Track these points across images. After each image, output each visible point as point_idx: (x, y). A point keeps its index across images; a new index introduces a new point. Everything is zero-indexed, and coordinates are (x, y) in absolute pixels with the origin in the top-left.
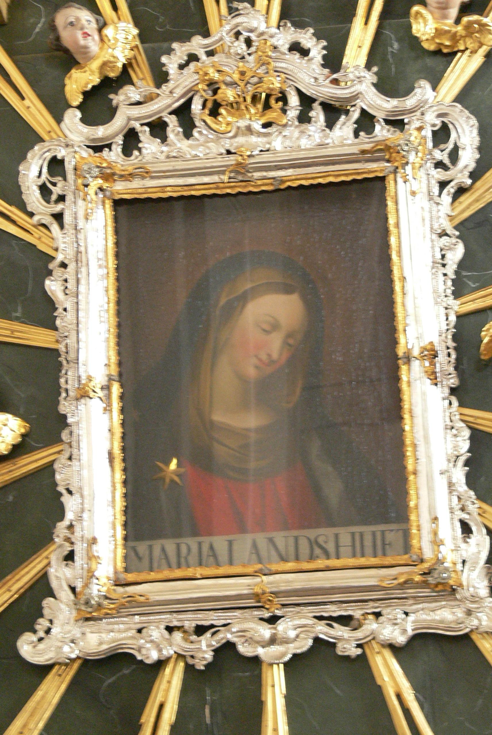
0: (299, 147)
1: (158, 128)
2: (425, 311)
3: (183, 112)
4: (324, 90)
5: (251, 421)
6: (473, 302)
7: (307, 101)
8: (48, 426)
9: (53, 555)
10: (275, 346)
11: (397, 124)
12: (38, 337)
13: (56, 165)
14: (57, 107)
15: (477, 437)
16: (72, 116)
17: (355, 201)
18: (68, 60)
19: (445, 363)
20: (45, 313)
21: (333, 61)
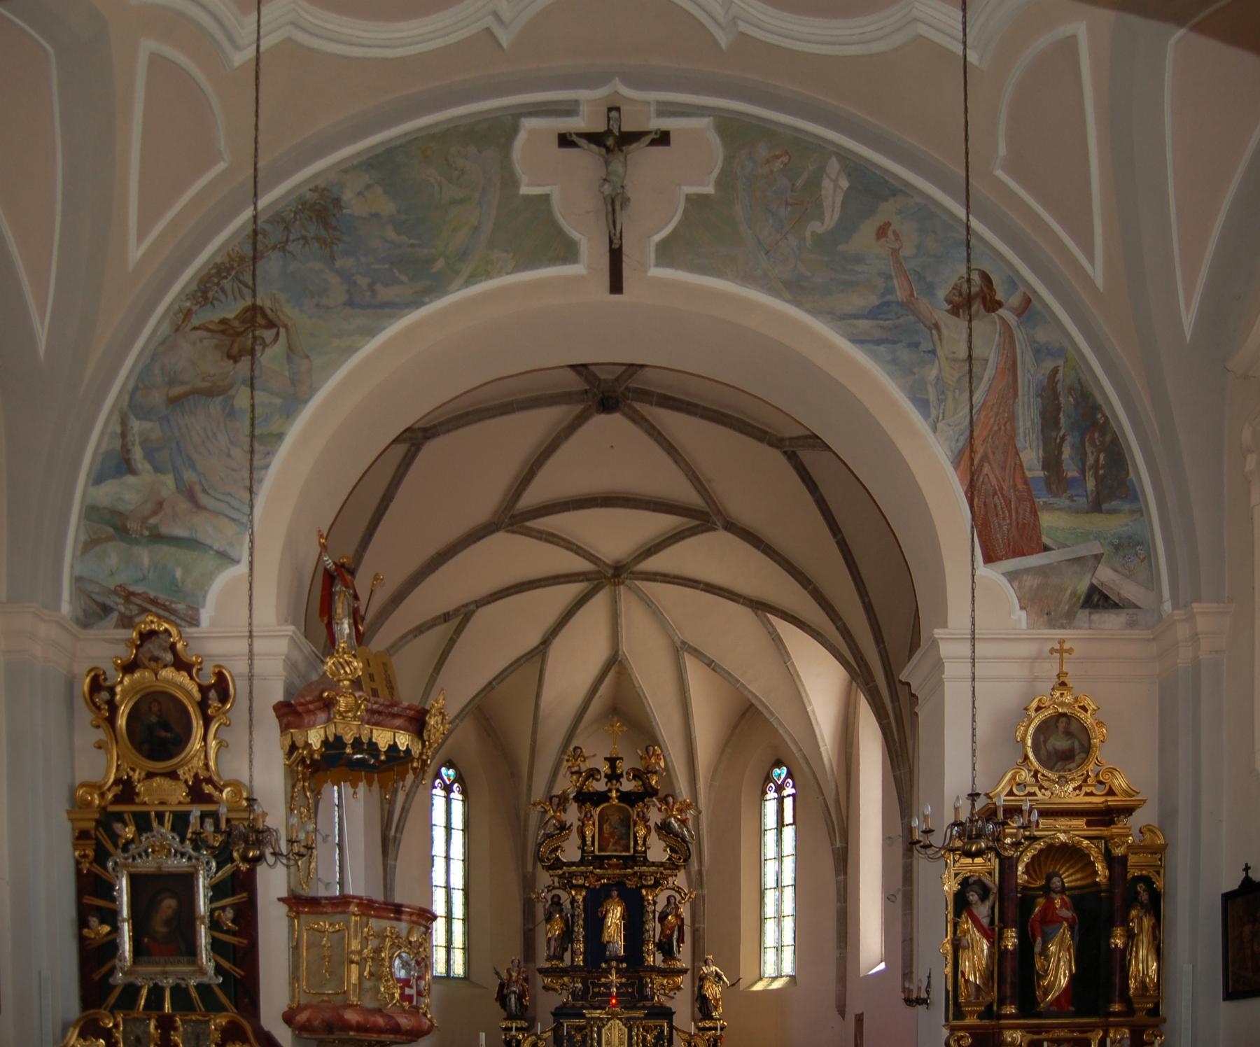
0: (177, 864)
1: (140, 856)
2: (202, 906)
3: (146, 852)
4: (180, 848)
5: (163, 930)
6: (214, 905)
7: (176, 852)
8: (116, 929)
9: (117, 961)
10: (170, 912)
11: (197, 859)
12: (110, 905)
13: (116, 863)
14: (116, 846)
15: (213, 938)
16: (119, 851)
17: (187, 880)
18: (118, 836)
19: (207, 921)
20: (113, 900)
21: (182, 841)
